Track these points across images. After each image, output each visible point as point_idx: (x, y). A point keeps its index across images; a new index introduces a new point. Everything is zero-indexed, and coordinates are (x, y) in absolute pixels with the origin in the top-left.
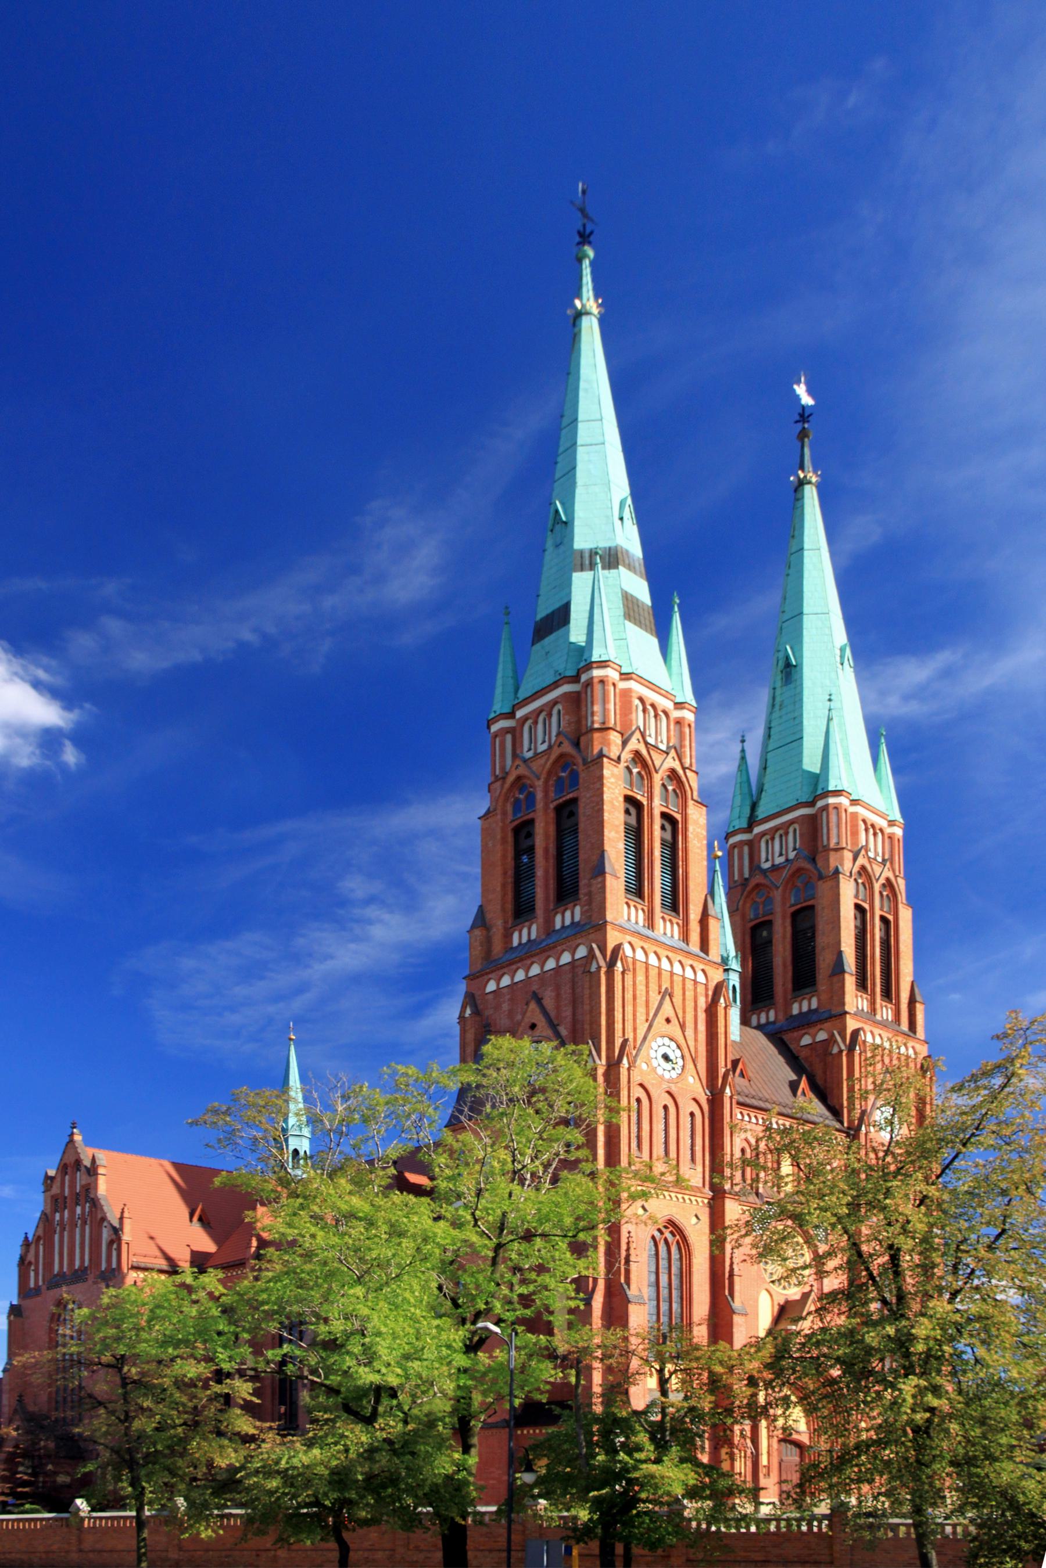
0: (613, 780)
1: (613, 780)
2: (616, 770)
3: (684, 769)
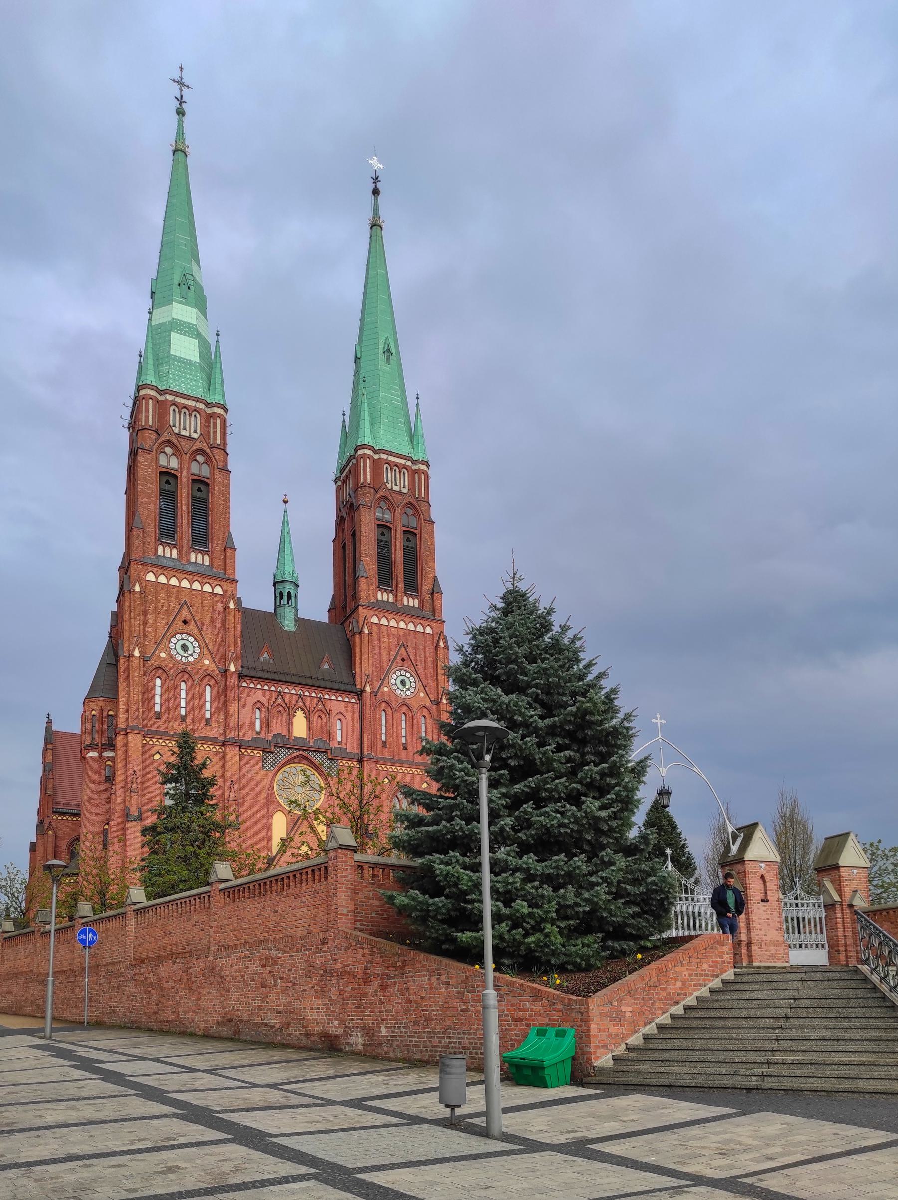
2: (148, 456)
3: (211, 448)
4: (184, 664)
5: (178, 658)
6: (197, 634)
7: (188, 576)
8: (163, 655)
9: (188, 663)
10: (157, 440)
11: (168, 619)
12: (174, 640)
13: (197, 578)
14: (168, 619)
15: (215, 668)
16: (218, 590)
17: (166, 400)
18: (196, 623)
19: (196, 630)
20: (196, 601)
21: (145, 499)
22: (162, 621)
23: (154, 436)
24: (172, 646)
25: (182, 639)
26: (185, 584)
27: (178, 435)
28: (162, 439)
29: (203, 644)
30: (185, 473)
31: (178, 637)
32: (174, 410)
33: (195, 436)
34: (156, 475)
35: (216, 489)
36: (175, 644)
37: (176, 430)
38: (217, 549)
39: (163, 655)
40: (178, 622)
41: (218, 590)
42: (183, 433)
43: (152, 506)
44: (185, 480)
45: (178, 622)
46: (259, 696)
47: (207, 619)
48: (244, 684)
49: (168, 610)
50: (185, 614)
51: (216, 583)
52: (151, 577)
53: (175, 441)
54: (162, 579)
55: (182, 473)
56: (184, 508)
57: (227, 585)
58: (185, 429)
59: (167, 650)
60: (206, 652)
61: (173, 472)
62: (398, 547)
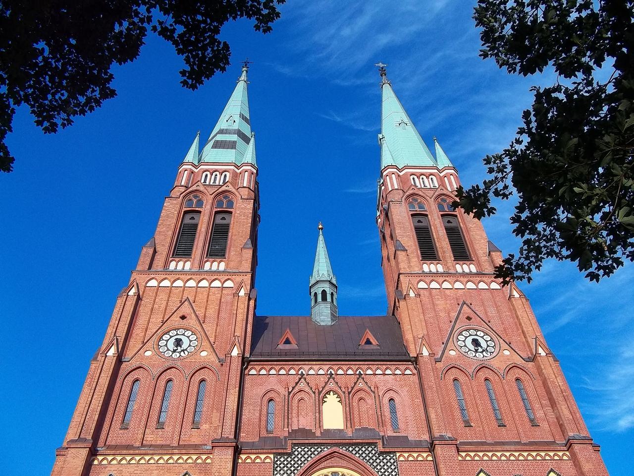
4: (174, 360)
11: (163, 318)
14: (163, 318)
16: (229, 284)
18: (197, 316)
31: (173, 333)
36: (167, 341)
40: (176, 318)
45: (176, 318)
47: (212, 312)
48: (253, 372)
50: (186, 309)
60: (206, 343)
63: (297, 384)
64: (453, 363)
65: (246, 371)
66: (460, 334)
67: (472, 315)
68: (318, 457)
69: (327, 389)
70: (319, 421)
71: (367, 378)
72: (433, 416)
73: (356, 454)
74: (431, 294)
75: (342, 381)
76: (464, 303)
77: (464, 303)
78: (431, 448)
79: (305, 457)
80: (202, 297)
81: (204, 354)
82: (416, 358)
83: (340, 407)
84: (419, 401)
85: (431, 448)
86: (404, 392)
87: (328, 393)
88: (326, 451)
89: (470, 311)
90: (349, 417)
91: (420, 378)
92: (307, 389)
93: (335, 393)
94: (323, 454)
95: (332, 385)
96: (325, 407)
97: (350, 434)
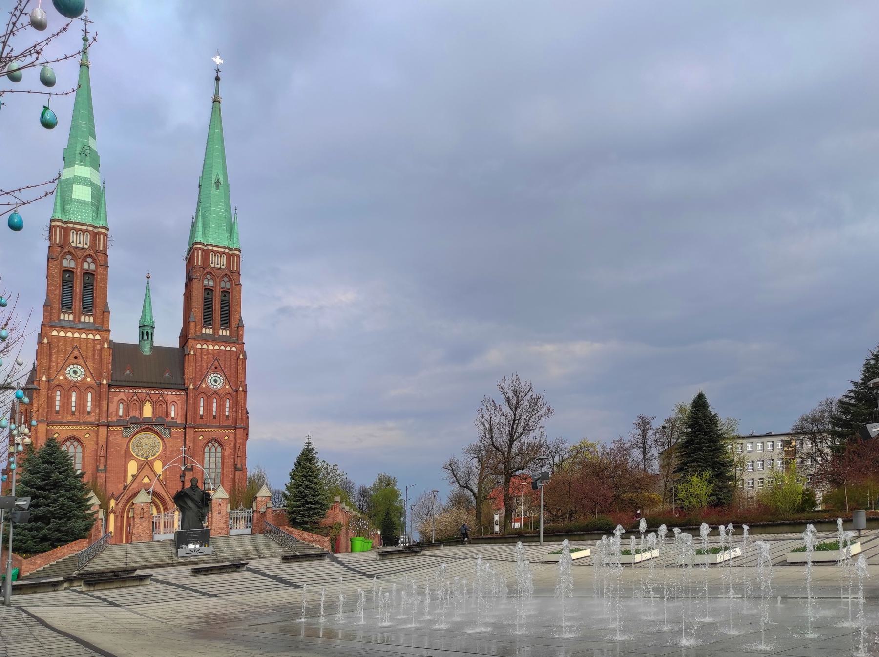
0: (54, 266)
1: (54, 266)
2: (55, 262)
4: (75, 382)
5: (71, 378)
6: (83, 363)
7: (78, 331)
8: (61, 378)
9: (77, 381)
10: (61, 252)
11: (65, 357)
12: (68, 369)
13: (84, 331)
14: (65, 357)
15: (94, 383)
16: (98, 337)
17: (68, 227)
18: (83, 358)
19: (83, 362)
20: (84, 345)
21: (52, 288)
22: (61, 358)
23: (59, 250)
24: (67, 372)
25: (74, 367)
26: (77, 335)
27: (76, 248)
28: (65, 251)
29: (87, 369)
30: (79, 270)
31: (71, 366)
32: (73, 232)
33: (86, 247)
34: (60, 273)
35: (99, 277)
36: (69, 371)
37: (74, 245)
38: (98, 313)
39: (61, 378)
40: (72, 358)
41: (98, 337)
42: (79, 246)
43: (57, 292)
44: (78, 274)
45: (72, 358)
46: (122, 396)
47: (90, 354)
48: (113, 390)
49: (65, 352)
50: (76, 353)
51: (96, 333)
52: (55, 333)
53: (73, 251)
54: (62, 334)
55: (77, 269)
56: (78, 290)
57: (104, 334)
58: (80, 243)
59: (64, 375)
61: (71, 270)
62: (217, 302)
63: (133, 397)
64: (203, 391)
65: (110, 390)
66: (210, 376)
67: (218, 367)
68: (140, 429)
69: (146, 400)
70: (141, 414)
71: (164, 396)
72: (188, 416)
73: (156, 428)
74: (202, 352)
75: (153, 396)
76: (216, 359)
77: (216, 359)
78: (185, 428)
79: (134, 428)
80: (84, 345)
81: (89, 379)
82: (187, 389)
83: (151, 408)
84: (185, 407)
85: (185, 428)
86: (179, 402)
87: (147, 401)
88: (144, 426)
89: (217, 364)
90: (154, 412)
91: (187, 397)
92: (138, 400)
93: (150, 401)
94: (142, 428)
95: (148, 398)
96: (144, 407)
97: (154, 420)
